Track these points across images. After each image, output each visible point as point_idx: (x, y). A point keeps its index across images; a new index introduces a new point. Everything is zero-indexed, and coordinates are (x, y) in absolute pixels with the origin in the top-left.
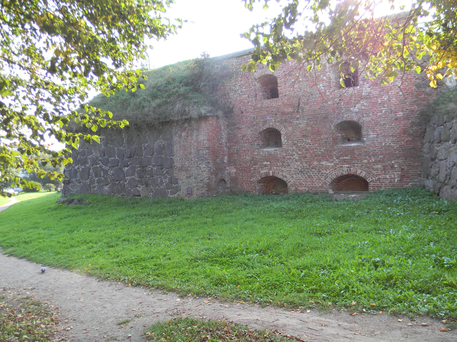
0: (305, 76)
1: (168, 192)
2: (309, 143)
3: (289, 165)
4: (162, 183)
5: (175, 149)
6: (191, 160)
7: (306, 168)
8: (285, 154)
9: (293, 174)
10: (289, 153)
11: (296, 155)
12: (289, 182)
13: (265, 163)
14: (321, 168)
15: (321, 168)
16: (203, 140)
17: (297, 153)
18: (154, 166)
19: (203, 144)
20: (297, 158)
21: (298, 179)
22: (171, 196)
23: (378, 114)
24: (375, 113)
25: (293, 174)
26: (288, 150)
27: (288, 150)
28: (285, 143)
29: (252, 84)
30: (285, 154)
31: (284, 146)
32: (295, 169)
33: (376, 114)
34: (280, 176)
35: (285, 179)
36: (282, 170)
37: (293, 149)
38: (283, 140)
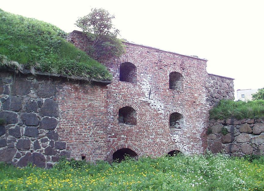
0: (155, 74)
1: (50, 159)
2: (155, 124)
3: (141, 140)
4: (37, 146)
5: (60, 110)
6: (86, 125)
7: (152, 144)
8: (138, 131)
9: (142, 148)
10: (141, 130)
11: (146, 132)
12: (139, 154)
13: (123, 136)
14: (161, 144)
15: (161, 144)
16: (99, 106)
17: (147, 131)
18: (20, 125)
19: (100, 110)
20: (146, 135)
21: (146, 152)
22: (53, 163)
23: (191, 112)
24: (190, 111)
25: (142, 148)
26: (140, 128)
27: (140, 128)
28: (139, 121)
29: (118, 66)
30: (138, 131)
31: (138, 124)
32: (145, 143)
33: (190, 112)
34: (134, 150)
35: (136, 152)
36: (135, 144)
37: (144, 128)
38: (138, 118)
